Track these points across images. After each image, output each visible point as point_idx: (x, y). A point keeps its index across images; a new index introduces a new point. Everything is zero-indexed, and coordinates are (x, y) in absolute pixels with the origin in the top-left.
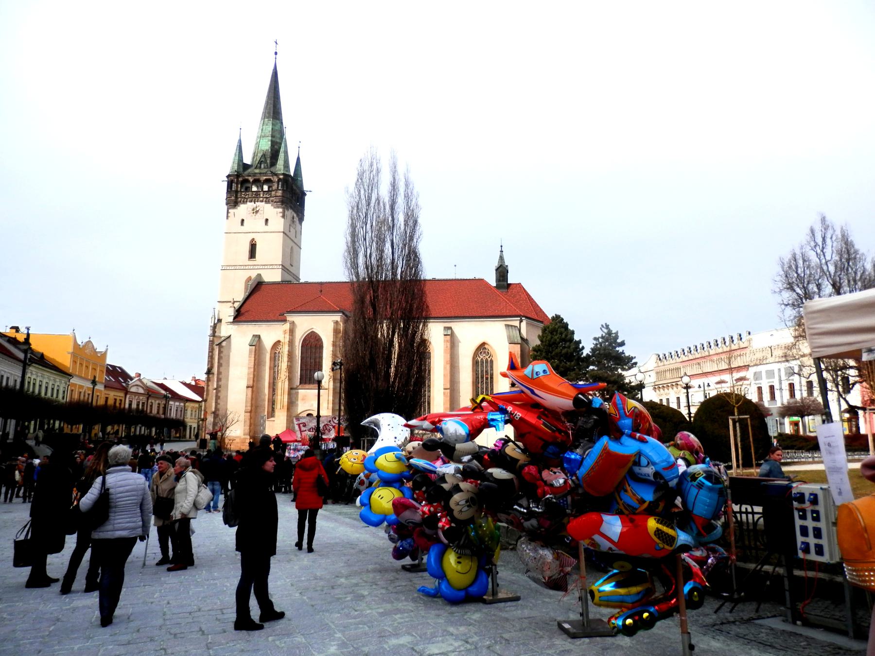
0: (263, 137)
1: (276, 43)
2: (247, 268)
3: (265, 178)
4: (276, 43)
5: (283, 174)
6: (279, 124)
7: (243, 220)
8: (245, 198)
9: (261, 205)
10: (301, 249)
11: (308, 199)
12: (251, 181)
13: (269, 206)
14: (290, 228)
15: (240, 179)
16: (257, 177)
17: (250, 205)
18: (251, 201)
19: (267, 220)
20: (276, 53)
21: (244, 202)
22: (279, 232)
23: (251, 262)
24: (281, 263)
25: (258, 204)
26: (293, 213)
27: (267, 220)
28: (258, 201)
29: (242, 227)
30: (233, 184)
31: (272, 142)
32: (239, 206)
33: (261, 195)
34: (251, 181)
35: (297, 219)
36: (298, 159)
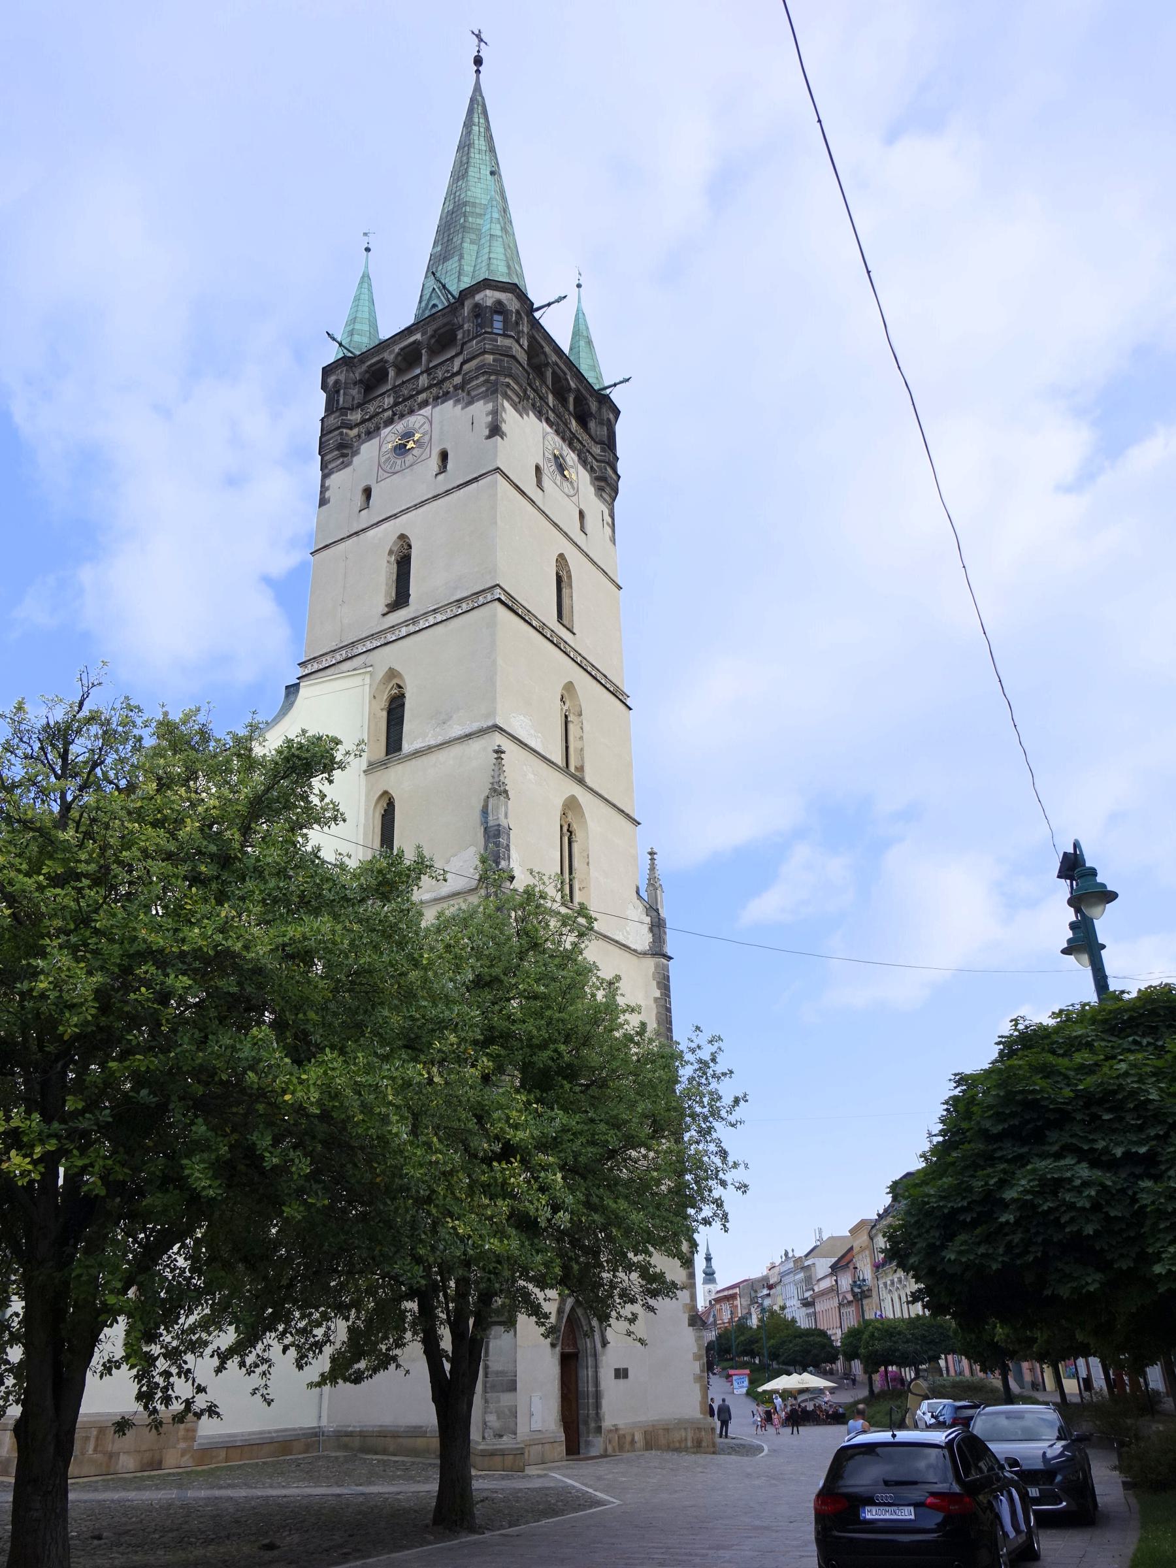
1: (478, 36)
4: (478, 36)
17: (390, 436)
19: (444, 456)
20: (478, 61)
27: (444, 456)
32: (356, 453)
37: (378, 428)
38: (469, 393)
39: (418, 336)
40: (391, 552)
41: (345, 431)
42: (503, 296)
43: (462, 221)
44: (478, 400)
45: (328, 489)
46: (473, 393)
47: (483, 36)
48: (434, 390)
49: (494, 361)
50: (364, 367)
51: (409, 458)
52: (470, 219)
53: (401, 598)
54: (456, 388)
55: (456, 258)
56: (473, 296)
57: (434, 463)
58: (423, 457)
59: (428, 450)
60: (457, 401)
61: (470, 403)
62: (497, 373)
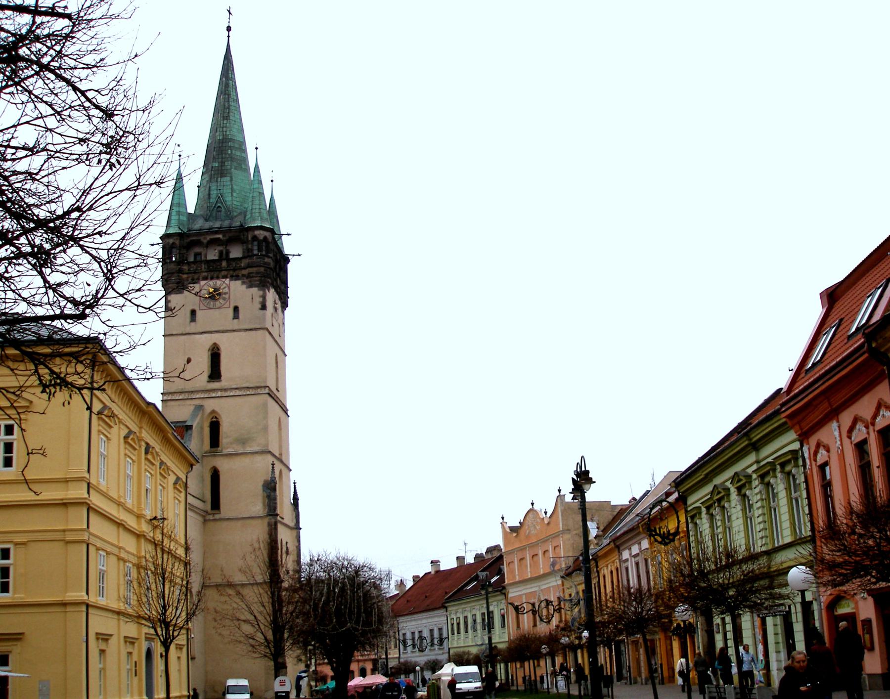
1: (230, 13)
7: (193, 313)
9: (223, 284)
10: (286, 355)
11: (293, 269)
13: (239, 282)
14: (272, 321)
17: (206, 286)
18: (205, 278)
19: (236, 309)
20: (229, 29)
21: (193, 279)
23: (215, 385)
25: (219, 282)
26: (275, 293)
27: (236, 309)
28: (218, 278)
29: (193, 324)
30: (174, 250)
34: (205, 241)
36: (272, 199)
37: (198, 279)
38: (250, 281)
39: (220, 236)
40: (209, 351)
41: (180, 275)
42: (267, 234)
43: (229, 152)
44: (255, 287)
45: (170, 301)
46: (253, 283)
47: (231, 12)
48: (231, 272)
49: (265, 270)
50: (188, 240)
51: (218, 304)
52: (233, 151)
53: (215, 374)
54: (243, 275)
55: (228, 179)
56: (254, 231)
57: (231, 312)
58: (224, 306)
59: (228, 303)
60: (243, 283)
61: (250, 286)
62: (265, 277)
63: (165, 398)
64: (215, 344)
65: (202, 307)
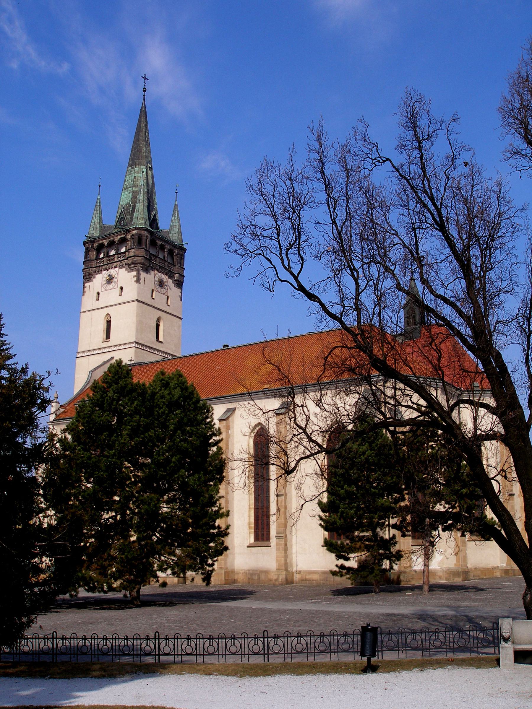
0: (125, 189)
1: (145, 78)
2: (101, 351)
3: (119, 237)
5: (136, 228)
6: (145, 170)
7: (98, 294)
8: (99, 266)
12: (106, 244)
13: (124, 269)
15: (96, 245)
16: (112, 239)
19: (122, 288)
20: (145, 90)
21: (98, 271)
22: (132, 301)
24: (134, 340)
25: (113, 272)
26: (160, 274)
27: (122, 288)
28: (112, 268)
31: (133, 192)
32: (94, 277)
33: (116, 260)
34: (106, 244)
35: (170, 281)
37: (101, 271)
53: (108, 336)
57: (118, 290)
60: (126, 270)
63: (79, 356)
64: (108, 314)
65: (103, 290)
